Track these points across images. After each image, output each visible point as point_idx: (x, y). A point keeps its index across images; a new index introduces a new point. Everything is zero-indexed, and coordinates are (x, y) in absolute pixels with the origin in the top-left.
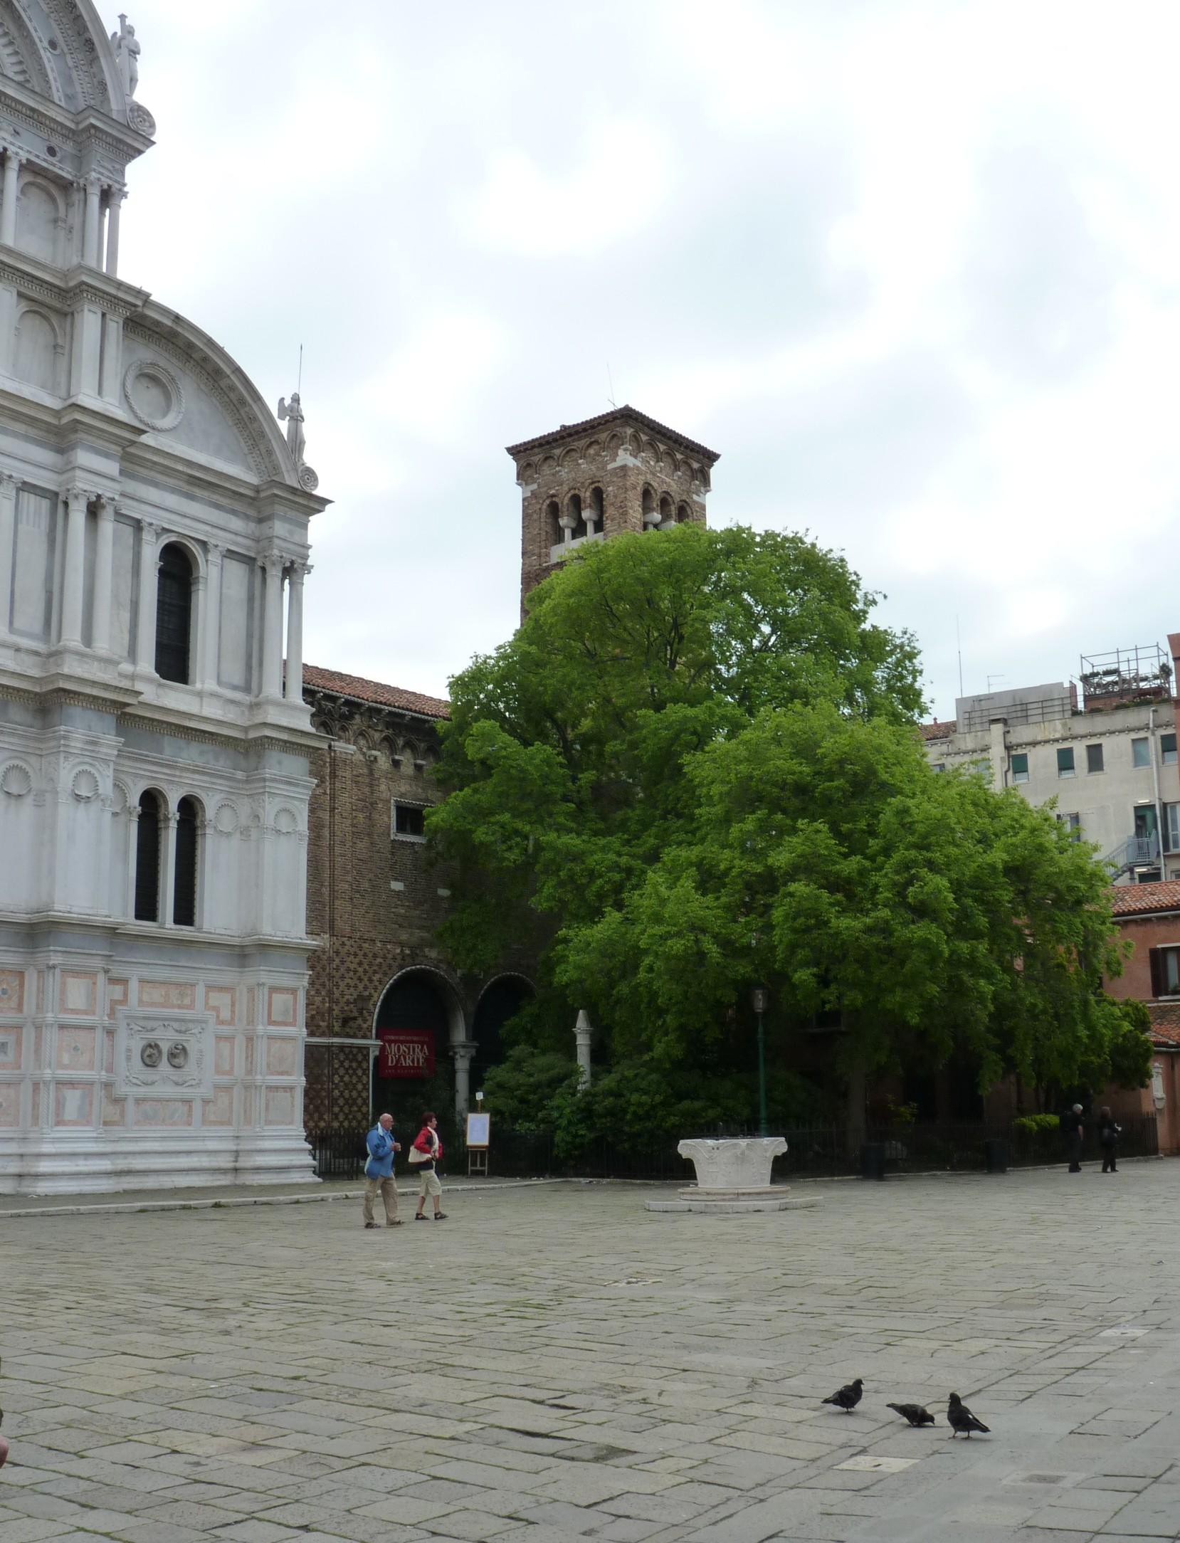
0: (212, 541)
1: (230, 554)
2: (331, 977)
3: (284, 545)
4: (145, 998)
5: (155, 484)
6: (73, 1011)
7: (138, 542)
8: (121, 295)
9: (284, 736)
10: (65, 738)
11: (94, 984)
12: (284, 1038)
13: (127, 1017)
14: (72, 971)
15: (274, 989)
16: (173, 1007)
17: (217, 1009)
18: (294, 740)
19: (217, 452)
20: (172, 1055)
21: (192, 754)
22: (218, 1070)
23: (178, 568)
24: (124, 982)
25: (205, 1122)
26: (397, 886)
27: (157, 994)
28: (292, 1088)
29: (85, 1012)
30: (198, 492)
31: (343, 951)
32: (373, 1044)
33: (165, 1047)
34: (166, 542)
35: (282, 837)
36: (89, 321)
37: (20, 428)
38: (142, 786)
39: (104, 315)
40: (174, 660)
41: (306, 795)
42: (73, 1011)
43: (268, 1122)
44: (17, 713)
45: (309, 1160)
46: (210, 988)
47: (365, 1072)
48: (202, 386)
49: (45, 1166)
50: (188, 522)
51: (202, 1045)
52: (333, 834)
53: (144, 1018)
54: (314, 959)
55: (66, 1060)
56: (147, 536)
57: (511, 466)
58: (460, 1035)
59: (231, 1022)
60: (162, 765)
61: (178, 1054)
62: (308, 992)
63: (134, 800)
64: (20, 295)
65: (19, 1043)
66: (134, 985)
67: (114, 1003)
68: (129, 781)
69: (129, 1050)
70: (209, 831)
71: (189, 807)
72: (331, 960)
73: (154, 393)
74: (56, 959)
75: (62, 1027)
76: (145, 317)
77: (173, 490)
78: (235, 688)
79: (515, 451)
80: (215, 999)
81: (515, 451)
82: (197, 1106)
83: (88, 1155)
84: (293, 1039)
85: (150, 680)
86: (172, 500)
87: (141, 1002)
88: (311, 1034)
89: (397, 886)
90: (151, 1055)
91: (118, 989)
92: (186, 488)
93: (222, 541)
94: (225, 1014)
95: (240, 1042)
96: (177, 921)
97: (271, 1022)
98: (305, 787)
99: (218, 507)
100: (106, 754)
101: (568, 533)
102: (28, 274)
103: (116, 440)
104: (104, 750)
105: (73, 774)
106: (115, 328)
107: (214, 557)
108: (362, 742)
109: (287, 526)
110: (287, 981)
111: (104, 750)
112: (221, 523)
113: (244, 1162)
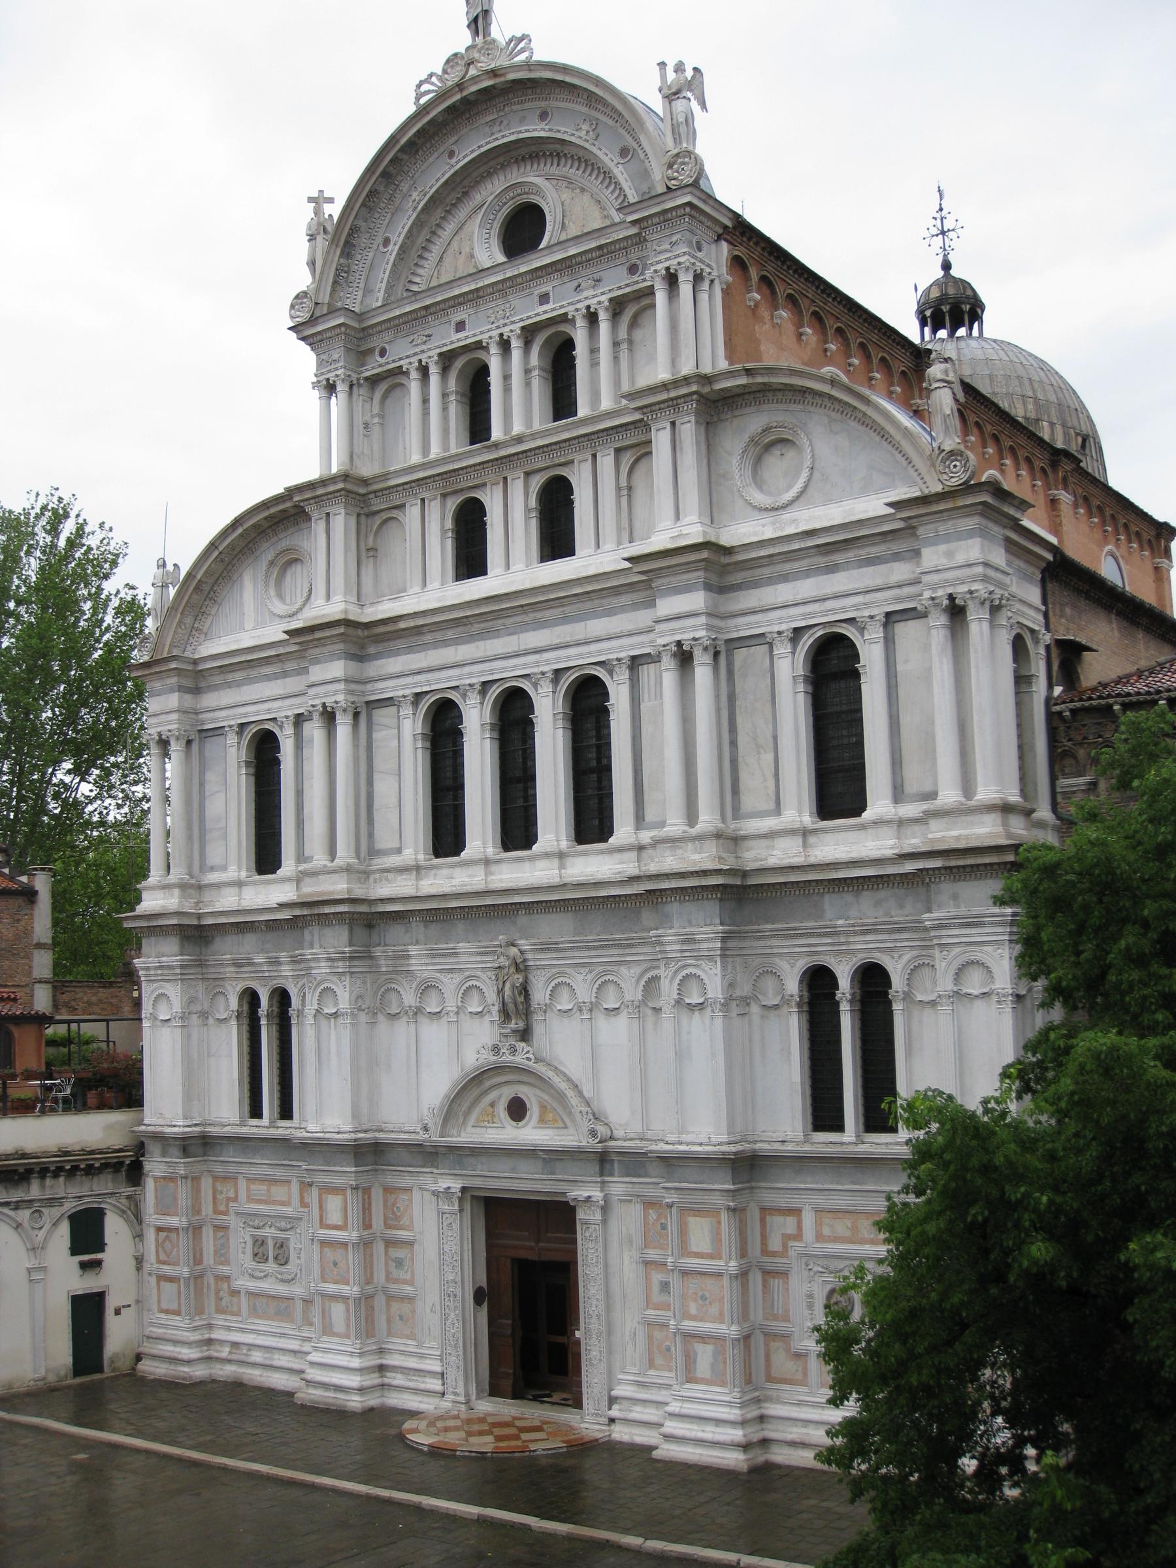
3: (936, 578)
4: (826, 1231)
5: (785, 578)
6: (697, 1255)
8: (673, 394)
9: (937, 863)
10: (660, 943)
11: (719, 1223)
13: (801, 1256)
14: (691, 1209)
16: (863, 1241)
18: (953, 863)
19: (866, 489)
21: (866, 908)
24: (796, 1212)
27: (842, 1227)
29: (711, 1256)
30: (839, 558)
34: (812, 640)
35: (978, 1004)
36: (661, 440)
37: (626, 599)
38: (802, 964)
39: (673, 424)
41: (1001, 933)
42: (697, 1255)
48: (833, 415)
50: (830, 604)
53: (825, 1257)
55: (693, 1309)
60: (819, 935)
63: (793, 986)
64: (618, 451)
66: (808, 1218)
67: (787, 1238)
68: (783, 965)
69: (810, 1296)
71: (873, 979)
73: (791, 454)
75: (685, 1273)
76: (722, 390)
77: (807, 574)
83: (718, 1422)
86: (807, 587)
87: (820, 1237)
91: (791, 1221)
92: (821, 561)
98: (992, 924)
99: (871, 562)
100: (709, 950)
102: (612, 428)
103: (689, 567)
104: (705, 945)
105: (677, 981)
106: (688, 429)
109: (942, 548)
111: (705, 945)
112: (878, 582)
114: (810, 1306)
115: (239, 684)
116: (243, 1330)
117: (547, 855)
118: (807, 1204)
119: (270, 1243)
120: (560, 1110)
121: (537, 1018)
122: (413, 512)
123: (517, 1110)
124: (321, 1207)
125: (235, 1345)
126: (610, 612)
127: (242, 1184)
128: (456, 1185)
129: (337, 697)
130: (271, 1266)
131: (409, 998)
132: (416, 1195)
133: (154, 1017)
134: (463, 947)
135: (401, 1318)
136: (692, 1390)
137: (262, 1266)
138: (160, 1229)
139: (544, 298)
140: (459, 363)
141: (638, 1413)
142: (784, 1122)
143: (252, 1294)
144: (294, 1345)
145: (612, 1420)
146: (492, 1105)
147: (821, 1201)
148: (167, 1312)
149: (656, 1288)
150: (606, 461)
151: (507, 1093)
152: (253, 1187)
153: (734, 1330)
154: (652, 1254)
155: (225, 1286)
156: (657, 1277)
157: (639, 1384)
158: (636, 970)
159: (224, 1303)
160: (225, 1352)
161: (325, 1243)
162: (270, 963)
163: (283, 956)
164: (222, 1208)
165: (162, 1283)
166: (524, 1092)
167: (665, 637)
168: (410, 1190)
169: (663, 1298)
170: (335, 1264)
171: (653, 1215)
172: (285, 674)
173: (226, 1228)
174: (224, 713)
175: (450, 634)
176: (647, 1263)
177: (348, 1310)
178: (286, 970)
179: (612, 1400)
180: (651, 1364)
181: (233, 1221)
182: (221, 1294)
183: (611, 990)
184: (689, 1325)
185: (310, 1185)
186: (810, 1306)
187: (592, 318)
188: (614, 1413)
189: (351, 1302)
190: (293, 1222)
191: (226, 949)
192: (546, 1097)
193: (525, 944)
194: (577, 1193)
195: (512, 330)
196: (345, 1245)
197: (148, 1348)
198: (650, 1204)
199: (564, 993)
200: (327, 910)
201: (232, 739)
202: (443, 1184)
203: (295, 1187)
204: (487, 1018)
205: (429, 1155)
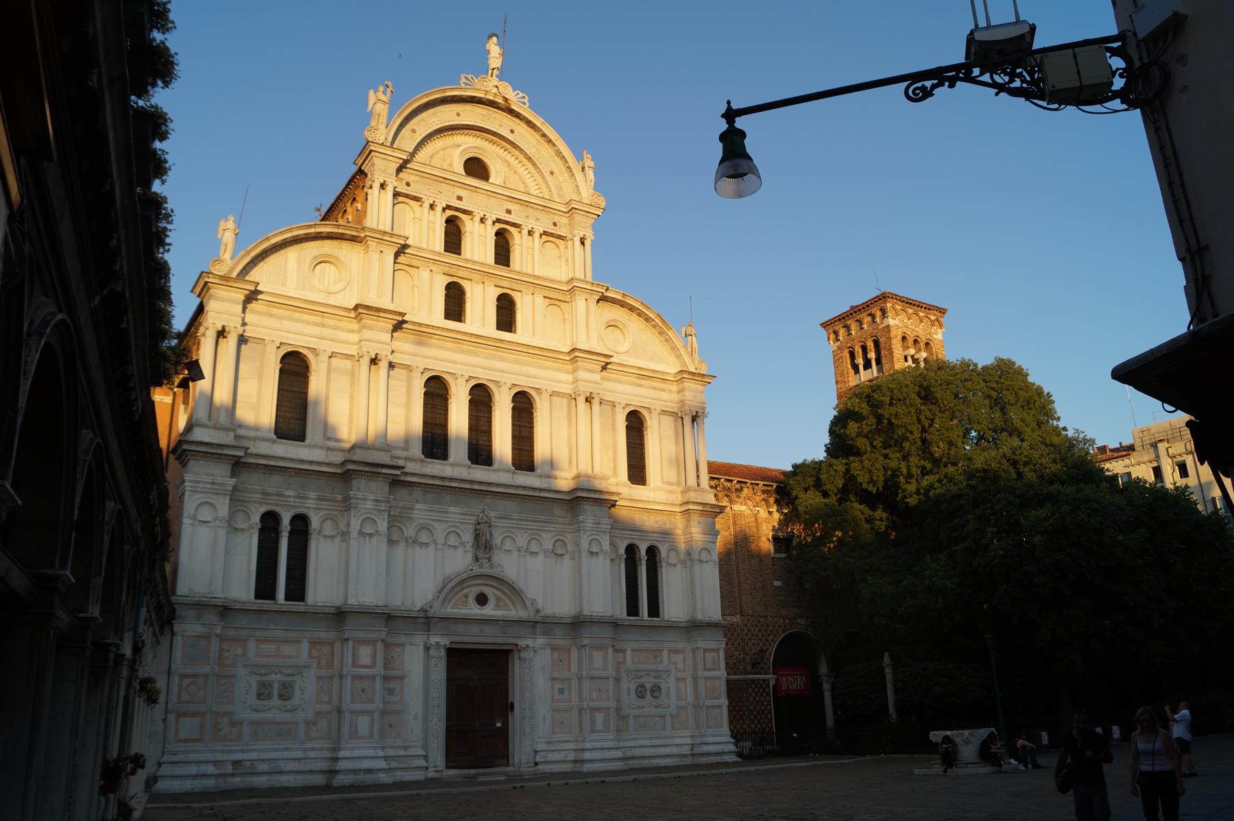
0: (653, 407)
1: (664, 412)
2: (743, 640)
5: (620, 382)
7: (614, 413)
12: (714, 678)
15: (706, 650)
17: (675, 663)
20: (652, 691)
22: (679, 698)
23: (635, 424)
24: (624, 651)
25: (673, 728)
26: (777, 584)
28: (720, 707)
30: (643, 382)
31: (749, 624)
32: (772, 678)
33: (648, 686)
38: (626, 543)
40: (637, 473)
43: (708, 727)
44: (558, 511)
45: (732, 748)
46: (671, 651)
47: (768, 694)
49: (587, 755)
51: (669, 684)
52: (737, 558)
54: (729, 632)
56: (619, 409)
57: (823, 332)
58: (824, 669)
59: (684, 671)
61: (656, 690)
62: (727, 651)
63: (622, 551)
65: (570, 688)
66: (629, 653)
68: (618, 541)
70: (664, 564)
72: (742, 630)
74: (586, 642)
75: (592, 678)
77: (630, 384)
78: (671, 484)
79: (825, 325)
80: (675, 658)
81: (825, 325)
82: (668, 719)
84: (719, 678)
85: (623, 485)
86: (629, 389)
87: (633, 662)
88: (728, 674)
89: (777, 584)
90: (641, 692)
91: (621, 655)
93: (658, 406)
94: (681, 666)
95: (689, 681)
96: (650, 616)
97: (706, 669)
99: (654, 388)
101: (861, 367)
107: (655, 414)
108: (750, 503)
110: (713, 645)
113: (697, 750)
114: (629, 694)
115: (280, 318)
116: (243, 751)
117: (508, 471)
118: (629, 646)
119: (276, 686)
120: (507, 600)
121: (495, 551)
122: (425, 273)
123: (482, 600)
124: (354, 655)
125: (236, 763)
126: (542, 367)
127: (252, 645)
128: (445, 641)
129: (384, 353)
130: (275, 701)
131: (410, 532)
132: (408, 648)
133: (194, 517)
134: (452, 509)
135: (390, 726)
136: (595, 736)
137: (265, 703)
138: (183, 676)
139: (509, 212)
140: (449, 213)
141: (551, 757)
142: (620, 611)
143: (252, 723)
144: (300, 754)
145: (536, 764)
146: (466, 597)
147: (634, 645)
148: (185, 741)
149: (556, 692)
150: (539, 299)
151: (475, 591)
152: (262, 646)
153: (614, 705)
154: (556, 675)
155: (226, 720)
156: (558, 686)
157: (548, 743)
158: (549, 535)
159: (222, 733)
160: (229, 769)
161: (355, 678)
162: (299, 497)
163: (312, 495)
164: (228, 662)
165: (182, 719)
166: (486, 590)
167: (585, 389)
168: (403, 645)
169: (561, 696)
170: (363, 691)
171: (556, 655)
172: (323, 326)
173: (234, 676)
174: (266, 330)
175: (450, 345)
176: (552, 679)
177: (372, 720)
178: (311, 503)
179: (536, 752)
180: (554, 733)
181: (241, 671)
182: (220, 726)
183: (534, 542)
184: (592, 704)
185: (347, 639)
186: (629, 694)
187: (530, 233)
188: (538, 759)
189: (376, 715)
190: (300, 670)
191: (254, 483)
192: (499, 593)
193: (493, 514)
194: (522, 643)
195: (491, 218)
196: (373, 678)
197: (166, 770)
198: (554, 649)
199: (508, 541)
200: (384, 471)
201: (271, 349)
202: (434, 639)
203: (305, 646)
204: (461, 549)
205: (425, 621)
